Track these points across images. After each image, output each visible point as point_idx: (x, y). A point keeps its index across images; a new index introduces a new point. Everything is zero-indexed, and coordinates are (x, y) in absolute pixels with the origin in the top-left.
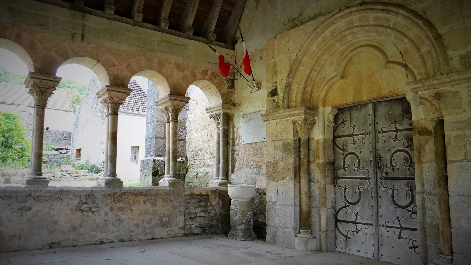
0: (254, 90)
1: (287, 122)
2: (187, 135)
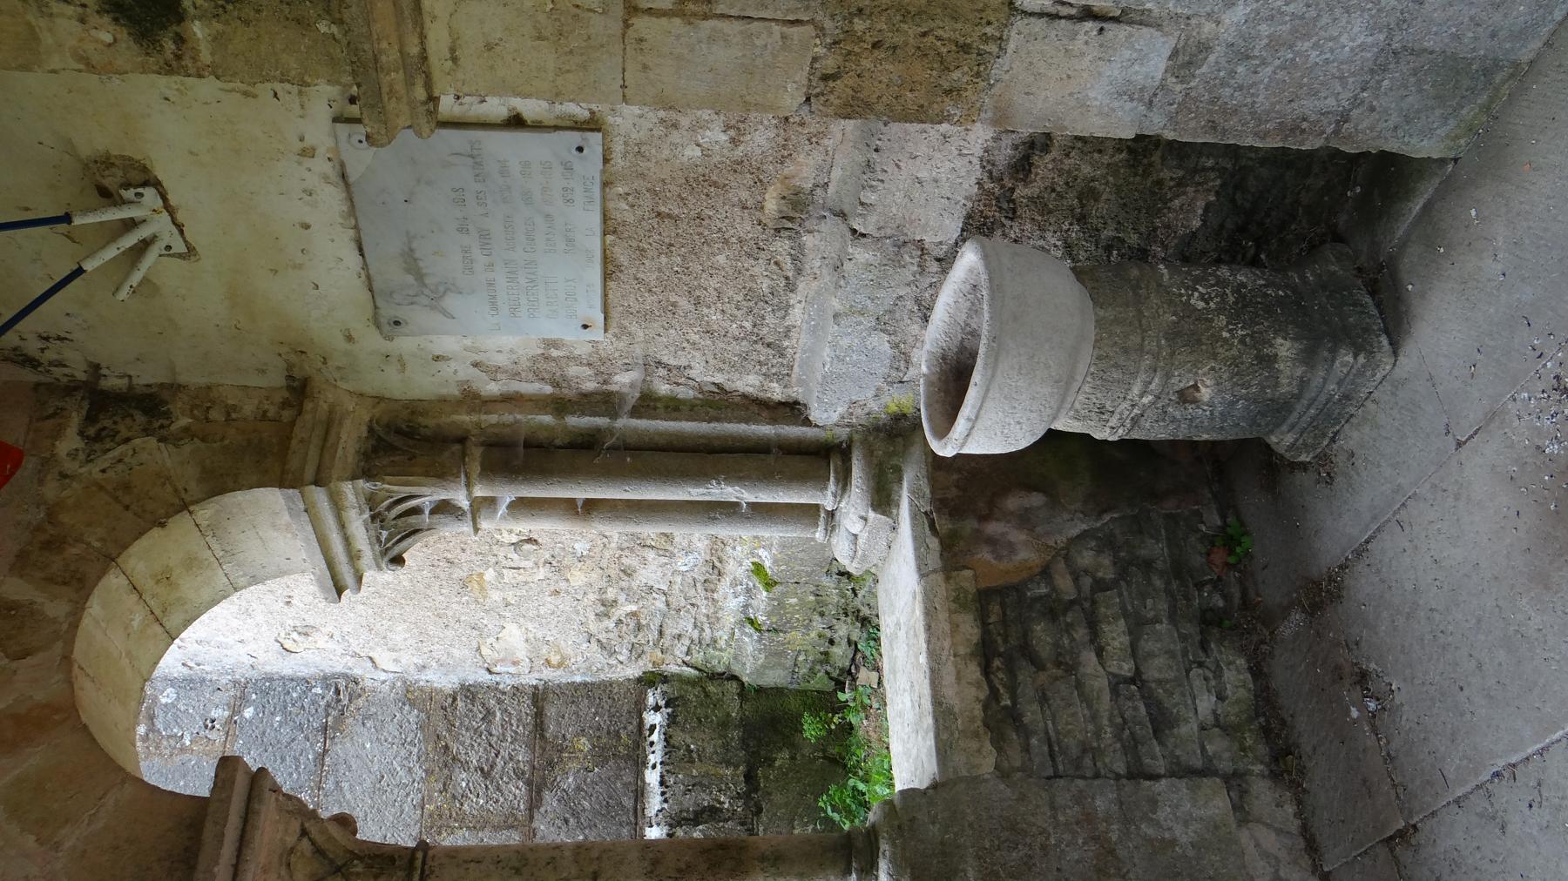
0: (160, 225)
2: (507, 683)
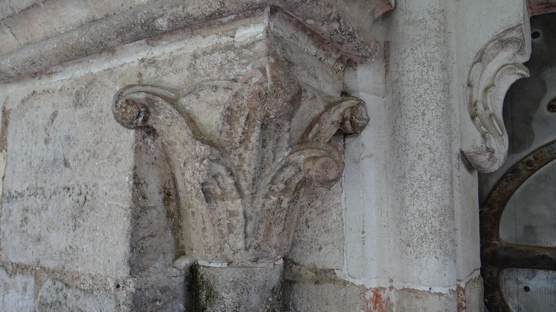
1: (78, 103)
